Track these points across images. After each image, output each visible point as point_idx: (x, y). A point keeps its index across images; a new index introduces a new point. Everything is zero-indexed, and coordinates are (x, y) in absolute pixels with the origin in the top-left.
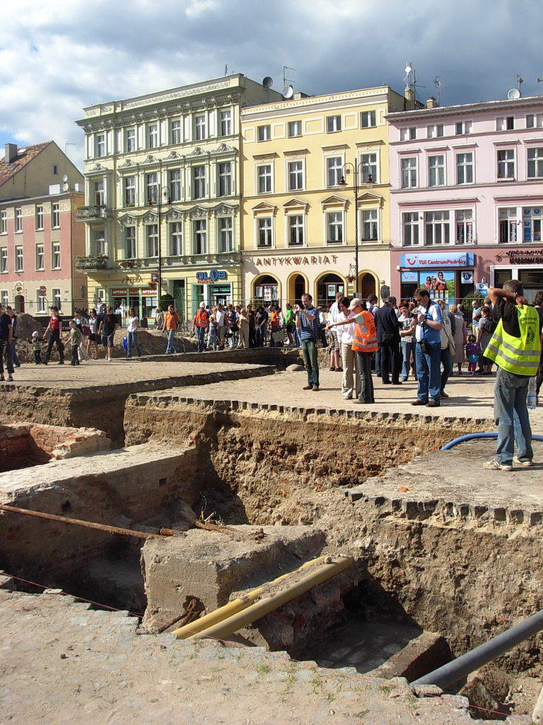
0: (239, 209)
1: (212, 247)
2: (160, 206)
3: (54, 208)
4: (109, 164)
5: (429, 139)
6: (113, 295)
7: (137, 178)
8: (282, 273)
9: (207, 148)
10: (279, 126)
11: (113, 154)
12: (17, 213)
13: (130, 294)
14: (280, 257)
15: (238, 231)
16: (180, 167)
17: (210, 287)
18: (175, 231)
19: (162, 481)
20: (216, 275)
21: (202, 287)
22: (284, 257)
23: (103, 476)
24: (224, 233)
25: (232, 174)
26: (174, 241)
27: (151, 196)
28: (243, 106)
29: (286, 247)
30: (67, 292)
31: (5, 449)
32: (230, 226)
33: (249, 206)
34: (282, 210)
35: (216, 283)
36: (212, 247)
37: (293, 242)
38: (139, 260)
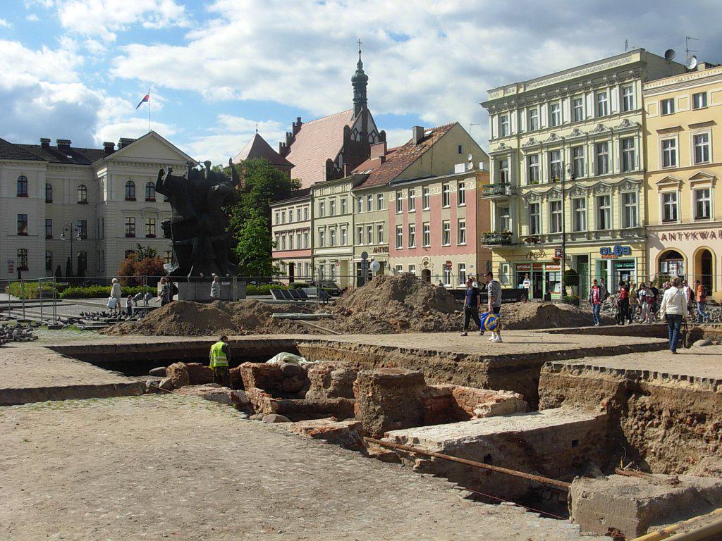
0: (644, 184)
1: (616, 222)
2: (564, 183)
3: (460, 186)
4: (513, 143)
6: (517, 269)
7: (540, 156)
8: (688, 247)
9: (609, 124)
10: (683, 99)
11: (516, 133)
12: (425, 191)
13: (534, 269)
14: (686, 232)
15: (642, 207)
16: (583, 143)
17: (614, 262)
18: (578, 207)
19: (575, 443)
20: (620, 251)
21: (606, 262)
22: (690, 231)
23: (521, 434)
24: (628, 209)
25: (636, 149)
26: (577, 217)
27: (554, 174)
28: (645, 81)
29: (692, 221)
30: (472, 266)
31: (429, 407)
32: (634, 202)
33: (653, 181)
35: (620, 258)
36: (616, 222)
37: (699, 216)
38: (543, 236)
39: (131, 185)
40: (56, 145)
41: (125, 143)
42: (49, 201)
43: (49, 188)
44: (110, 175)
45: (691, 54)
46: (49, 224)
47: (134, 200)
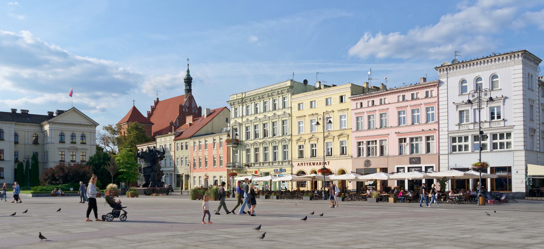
0: (291, 140)
1: (280, 158)
4: (239, 121)
5: (368, 106)
15: (290, 151)
28: (293, 94)
33: (295, 139)
34: (307, 141)
36: (280, 158)
39: (62, 135)
40: (20, 112)
41: (60, 112)
42: (16, 143)
43: (16, 135)
44: (51, 129)
45: (318, 81)
46: (16, 154)
47: (64, 142)
